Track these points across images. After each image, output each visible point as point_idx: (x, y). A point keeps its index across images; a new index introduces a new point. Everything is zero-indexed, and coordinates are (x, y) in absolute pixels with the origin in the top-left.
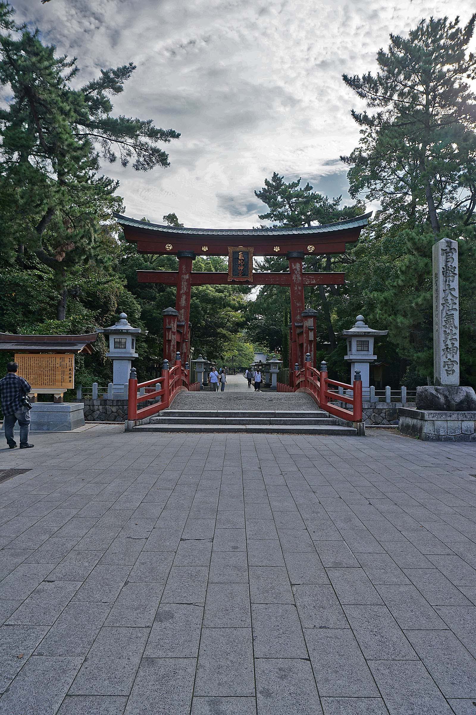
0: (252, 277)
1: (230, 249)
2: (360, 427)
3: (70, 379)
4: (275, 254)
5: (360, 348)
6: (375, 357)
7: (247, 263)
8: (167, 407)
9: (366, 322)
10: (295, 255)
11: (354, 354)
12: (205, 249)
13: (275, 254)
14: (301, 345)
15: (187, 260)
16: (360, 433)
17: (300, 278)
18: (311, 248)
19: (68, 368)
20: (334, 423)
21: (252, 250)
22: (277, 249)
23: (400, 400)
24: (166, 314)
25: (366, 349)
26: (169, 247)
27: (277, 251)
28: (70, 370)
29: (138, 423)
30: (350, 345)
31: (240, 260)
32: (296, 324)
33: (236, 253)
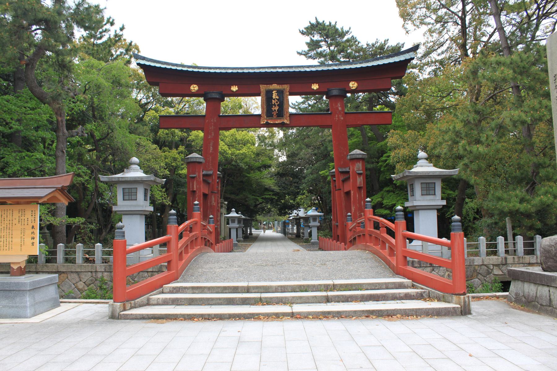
0: (288, 118)
1: (263, 88)
2: (465, 302)
3: (33, 241)
4: (314, 93)
5: (425, 192)
6: (444, 203)
7: (282, 103)
8: (175, 279)
9: (429, 159)
10: (335, 92)
11: (418, 199)
12: (234, 89)
13: (314, 93)
14: (348, 194)
15: (214, 101)
16: (465, 311)
17: (342, 118)
18: (353, 85)
19: (31, 225)
20: (420, 297)
21: (286, 87)
22: (315, 87)
23: (477, 254)
24: (189, 161)
25: (432, 192)
26: (194, 88)
27: (315, 88)
28: (33, 227)
29: (128, 306)
30: (412, 190)
31: (274, 99)
32: (340, 170)
33: (269, 94)
